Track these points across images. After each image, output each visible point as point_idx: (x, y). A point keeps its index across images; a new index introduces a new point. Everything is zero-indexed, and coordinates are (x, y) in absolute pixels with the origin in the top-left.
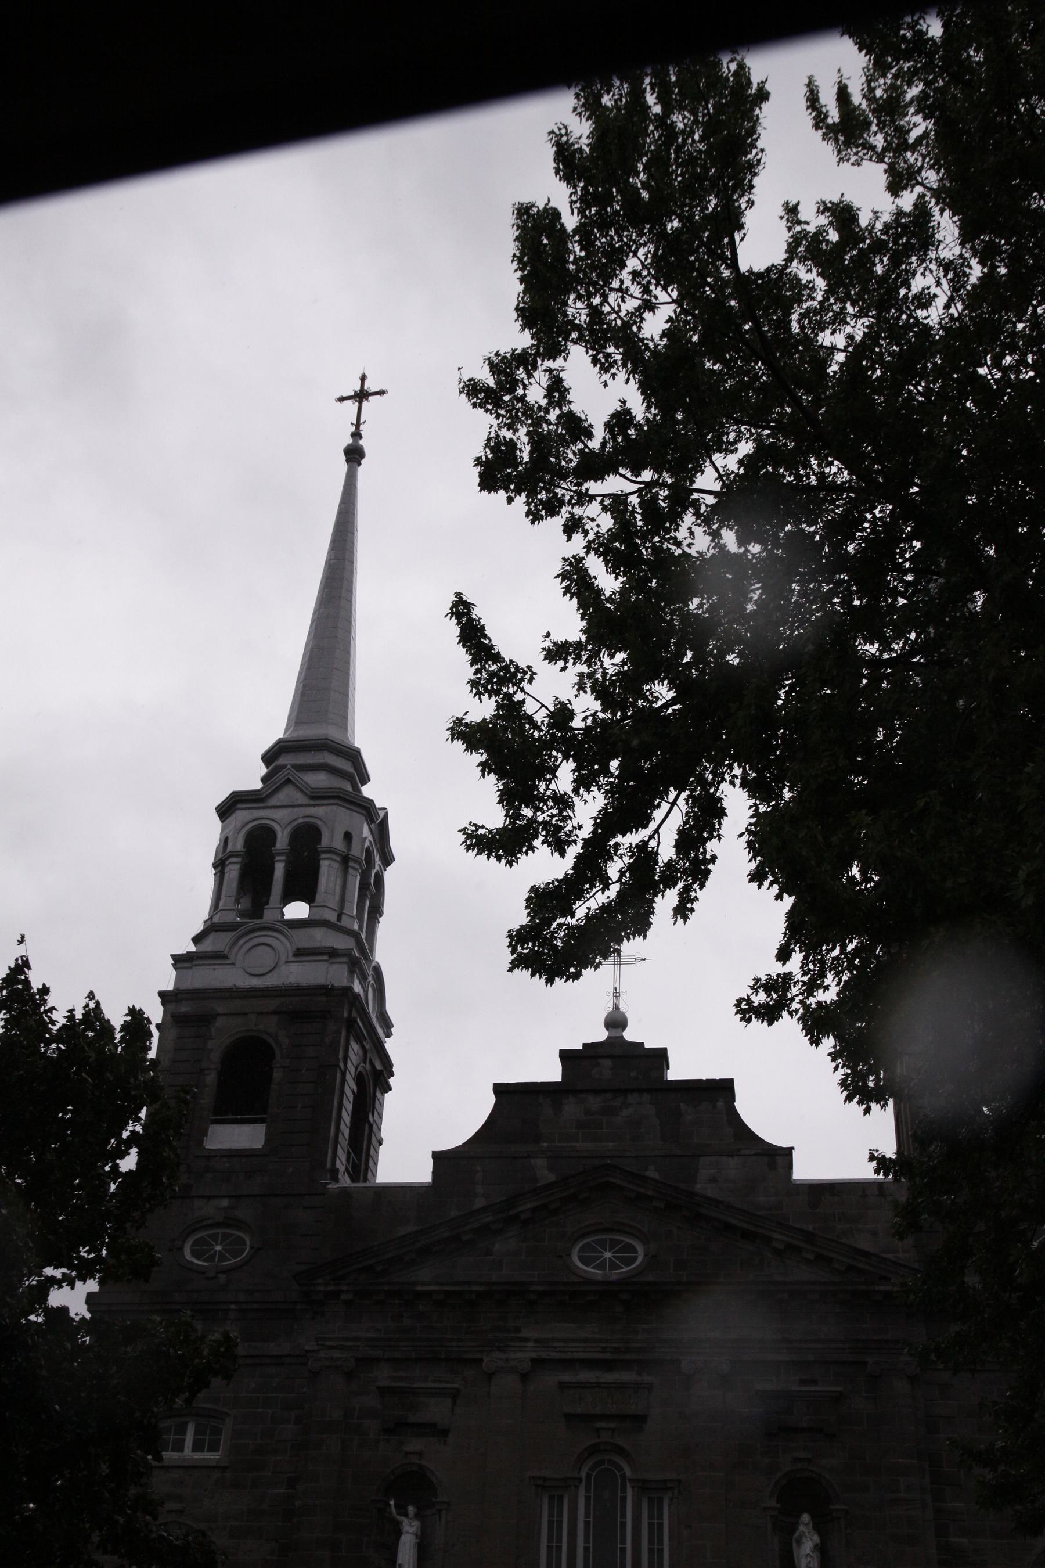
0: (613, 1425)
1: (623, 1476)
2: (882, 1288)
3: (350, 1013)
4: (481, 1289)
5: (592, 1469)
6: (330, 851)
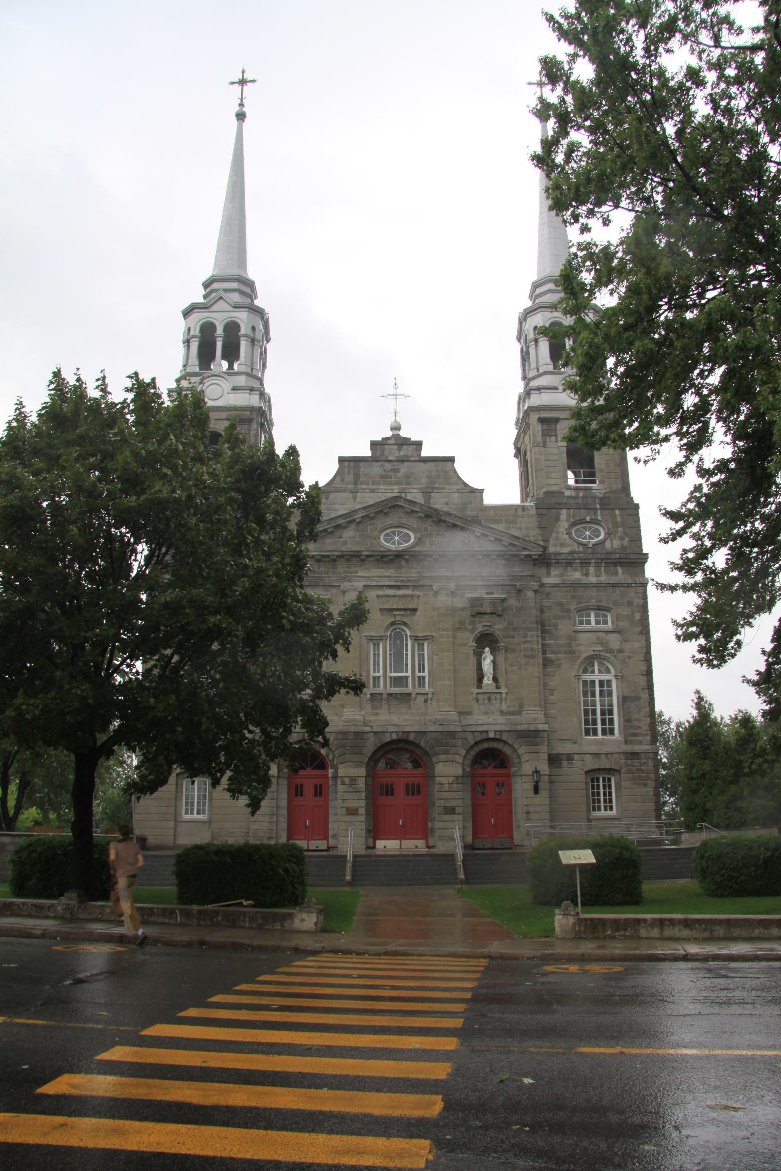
1: (406, 635)
6: (246, 336)
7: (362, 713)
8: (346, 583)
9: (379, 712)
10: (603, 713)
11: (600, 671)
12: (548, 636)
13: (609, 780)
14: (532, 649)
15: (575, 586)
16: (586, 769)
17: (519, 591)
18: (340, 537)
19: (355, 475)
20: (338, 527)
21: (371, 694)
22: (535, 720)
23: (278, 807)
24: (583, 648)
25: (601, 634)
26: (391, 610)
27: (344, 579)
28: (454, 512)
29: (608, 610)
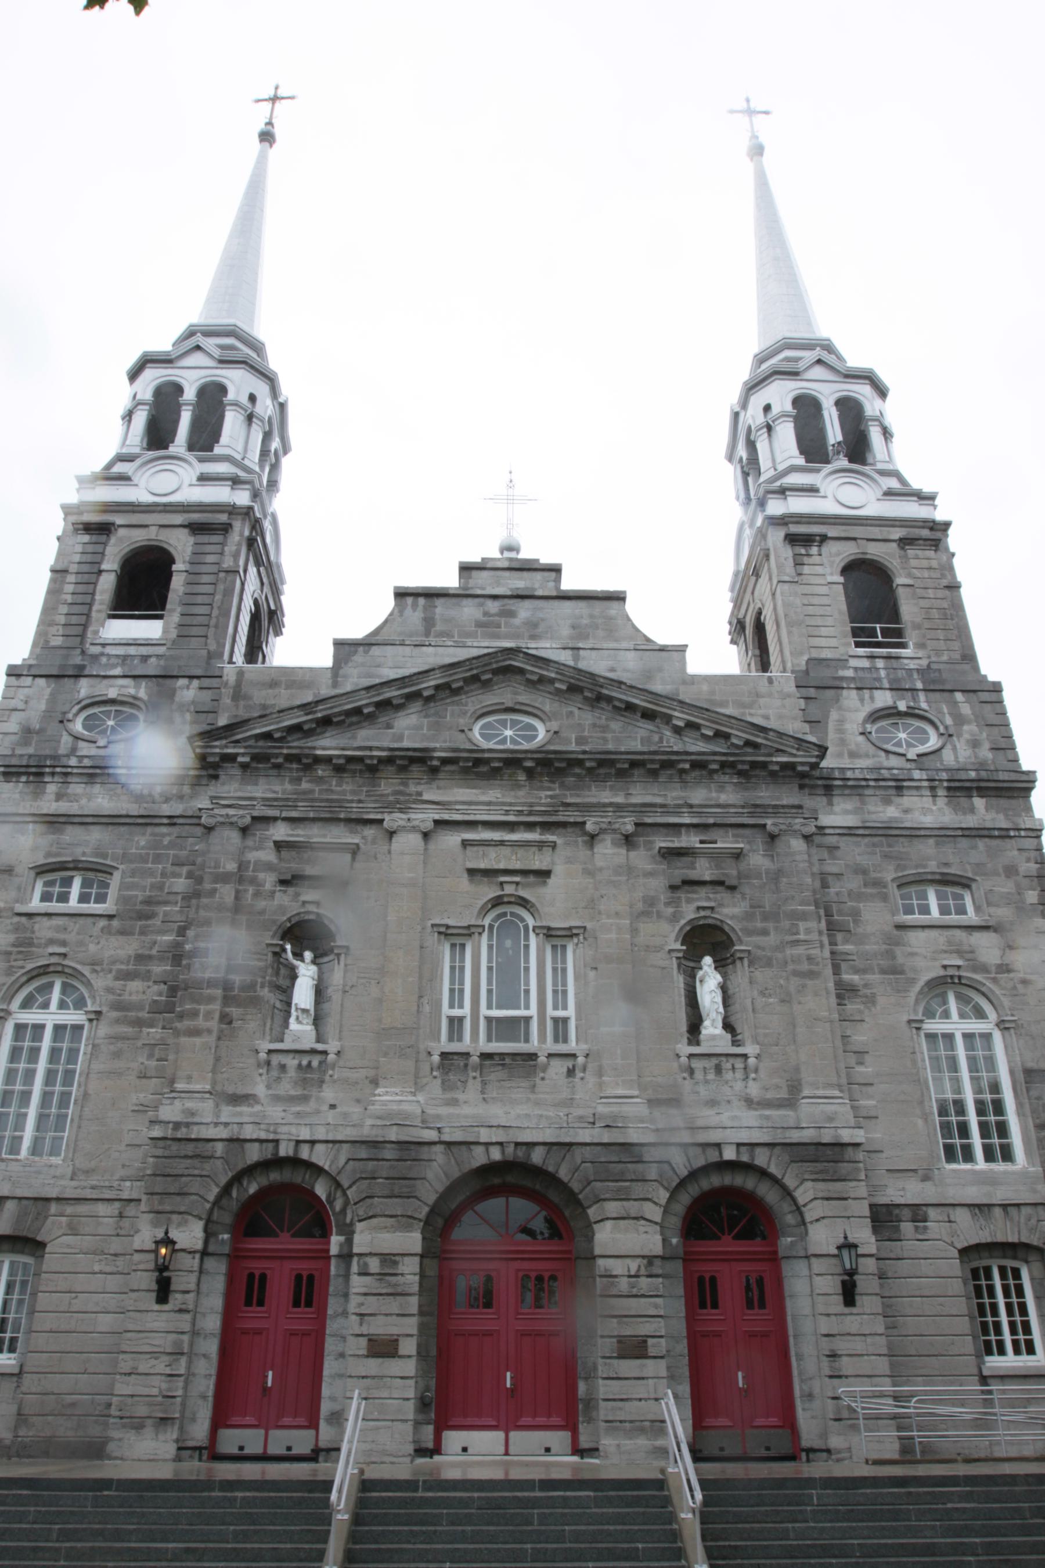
0: (517, 879)
1: (526, 928)
2: (780, 759)
3: (251, 532)
5: (495, 920)
6: (236, 404)
7: (420, 1098)
8: (397, 815)
9: (461, 1097)
11: (962, 1015)
12: (839, 937)
13: (1017, 1274)
14: (810, 959)
15: (888, 833)
16: (960, 1246)
17: (773, 837)
18: (389, 726)
19: (425, 619)
20: (385, 705)
21: (444, 1055)
22: (831, 1119)
23: (195, 1333)
24: (920, 963)
25: (958, 933)
26: (489, 873)
27: (390, 807)
28: (629, 682)
29: (964, 883)
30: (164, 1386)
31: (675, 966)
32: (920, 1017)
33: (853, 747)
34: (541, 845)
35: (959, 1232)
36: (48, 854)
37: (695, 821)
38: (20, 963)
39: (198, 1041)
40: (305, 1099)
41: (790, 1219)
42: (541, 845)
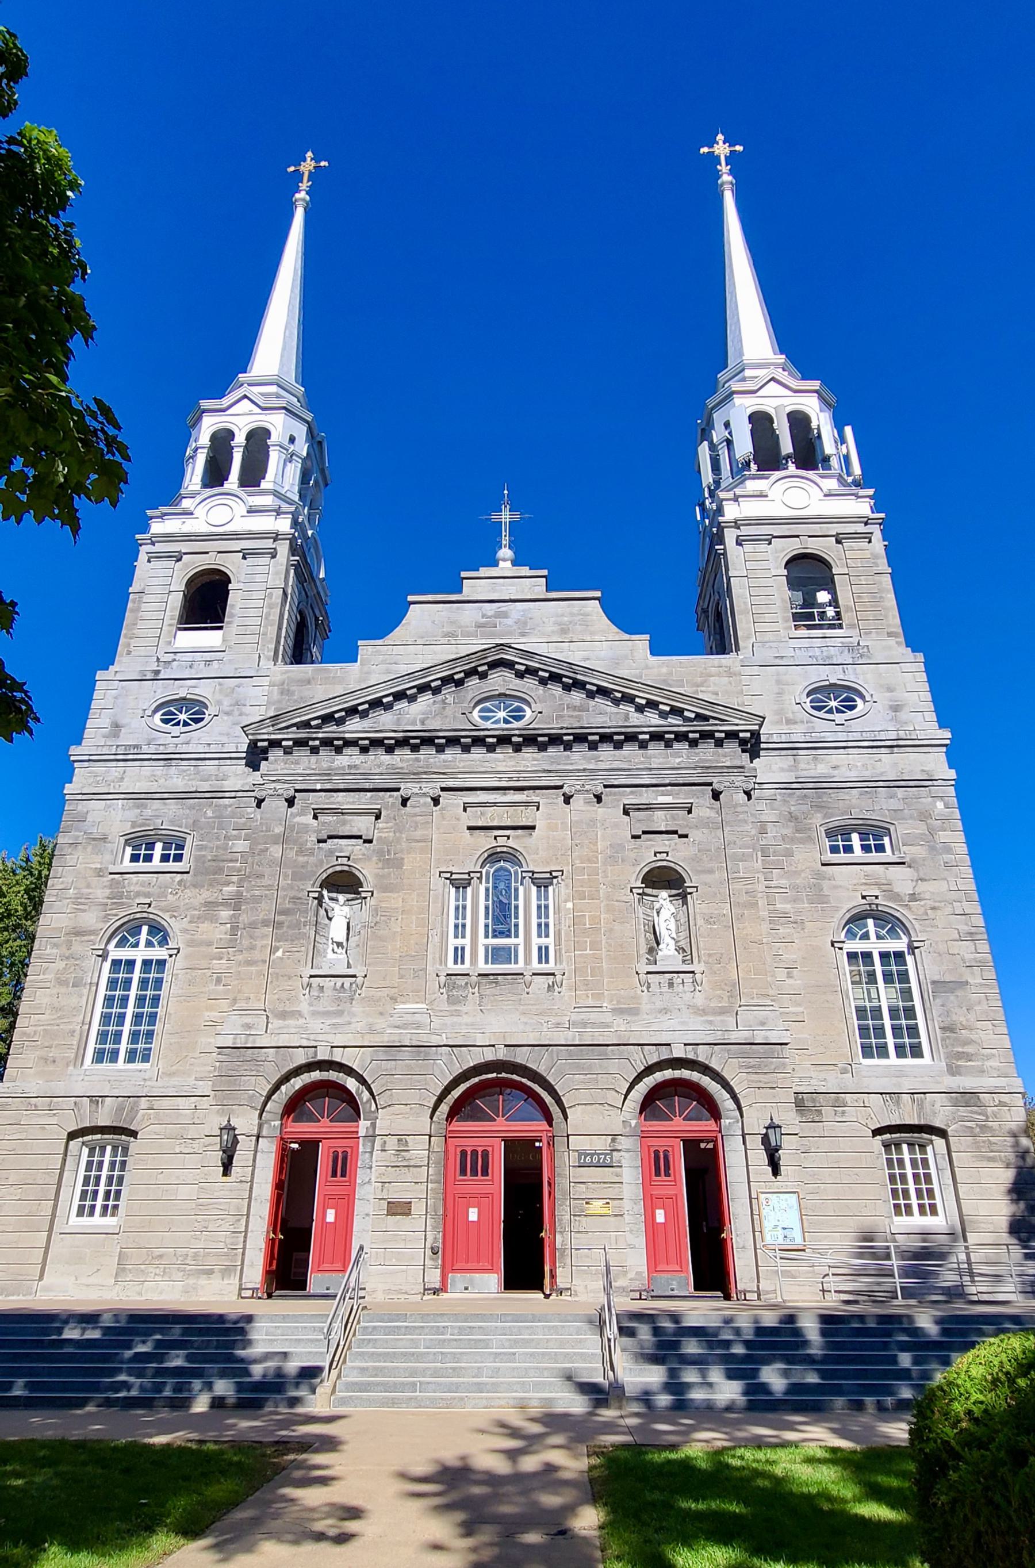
4: (401, 735)
9: (464, 1009)
10: (894, 1013)
11: (879, 937)
15: (820, 785)
30: (228, 1241)
31: (636, 900)
32: (842, 938)
33: (790, 716)
34: (527, 804)
35: (873, 1116)
36: (134, 824)
37: (654, 781)
38: (114, 912)
39: (253, 968)
40: (340, 1013)
41: (730, 1104)
42: (527, 804)
